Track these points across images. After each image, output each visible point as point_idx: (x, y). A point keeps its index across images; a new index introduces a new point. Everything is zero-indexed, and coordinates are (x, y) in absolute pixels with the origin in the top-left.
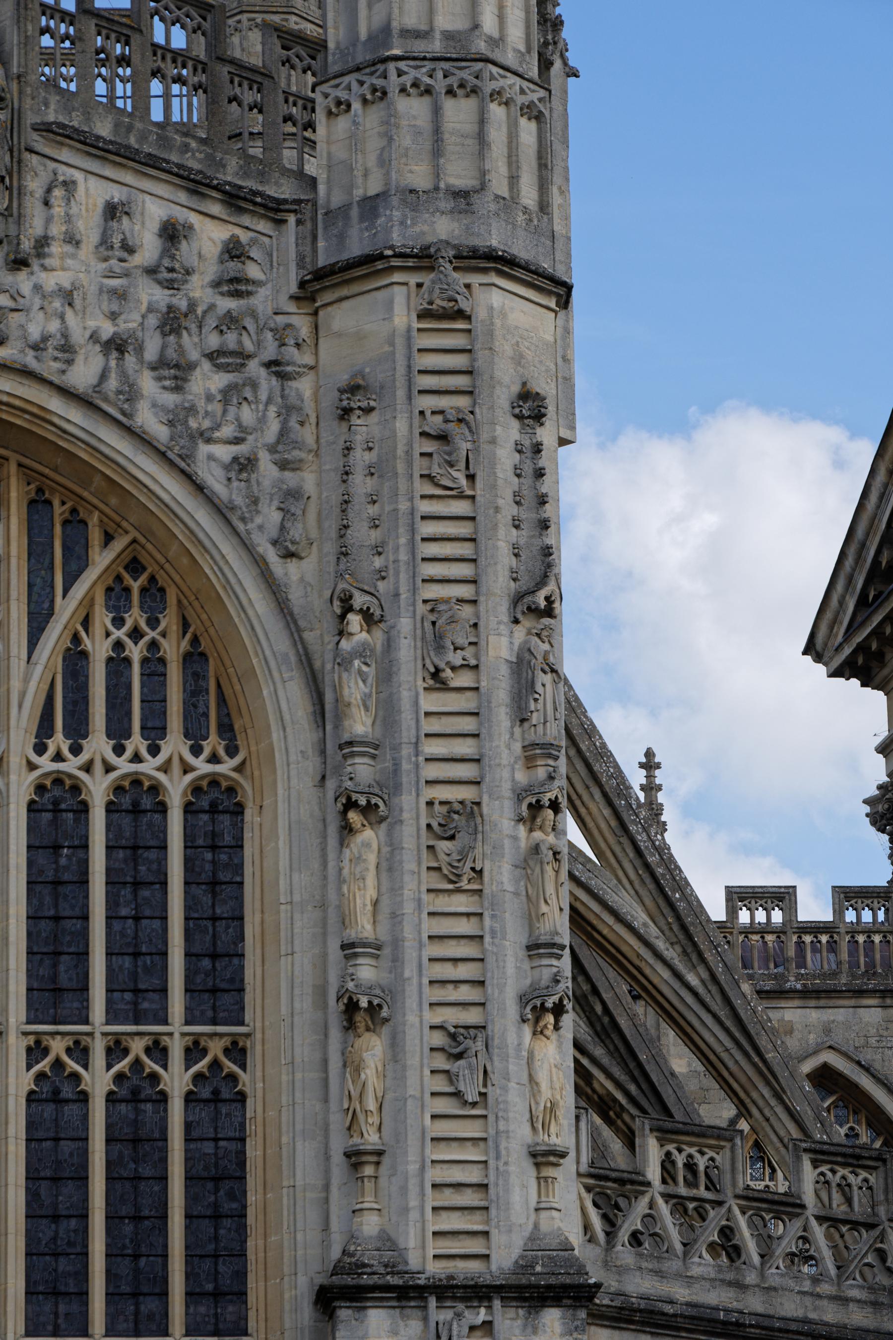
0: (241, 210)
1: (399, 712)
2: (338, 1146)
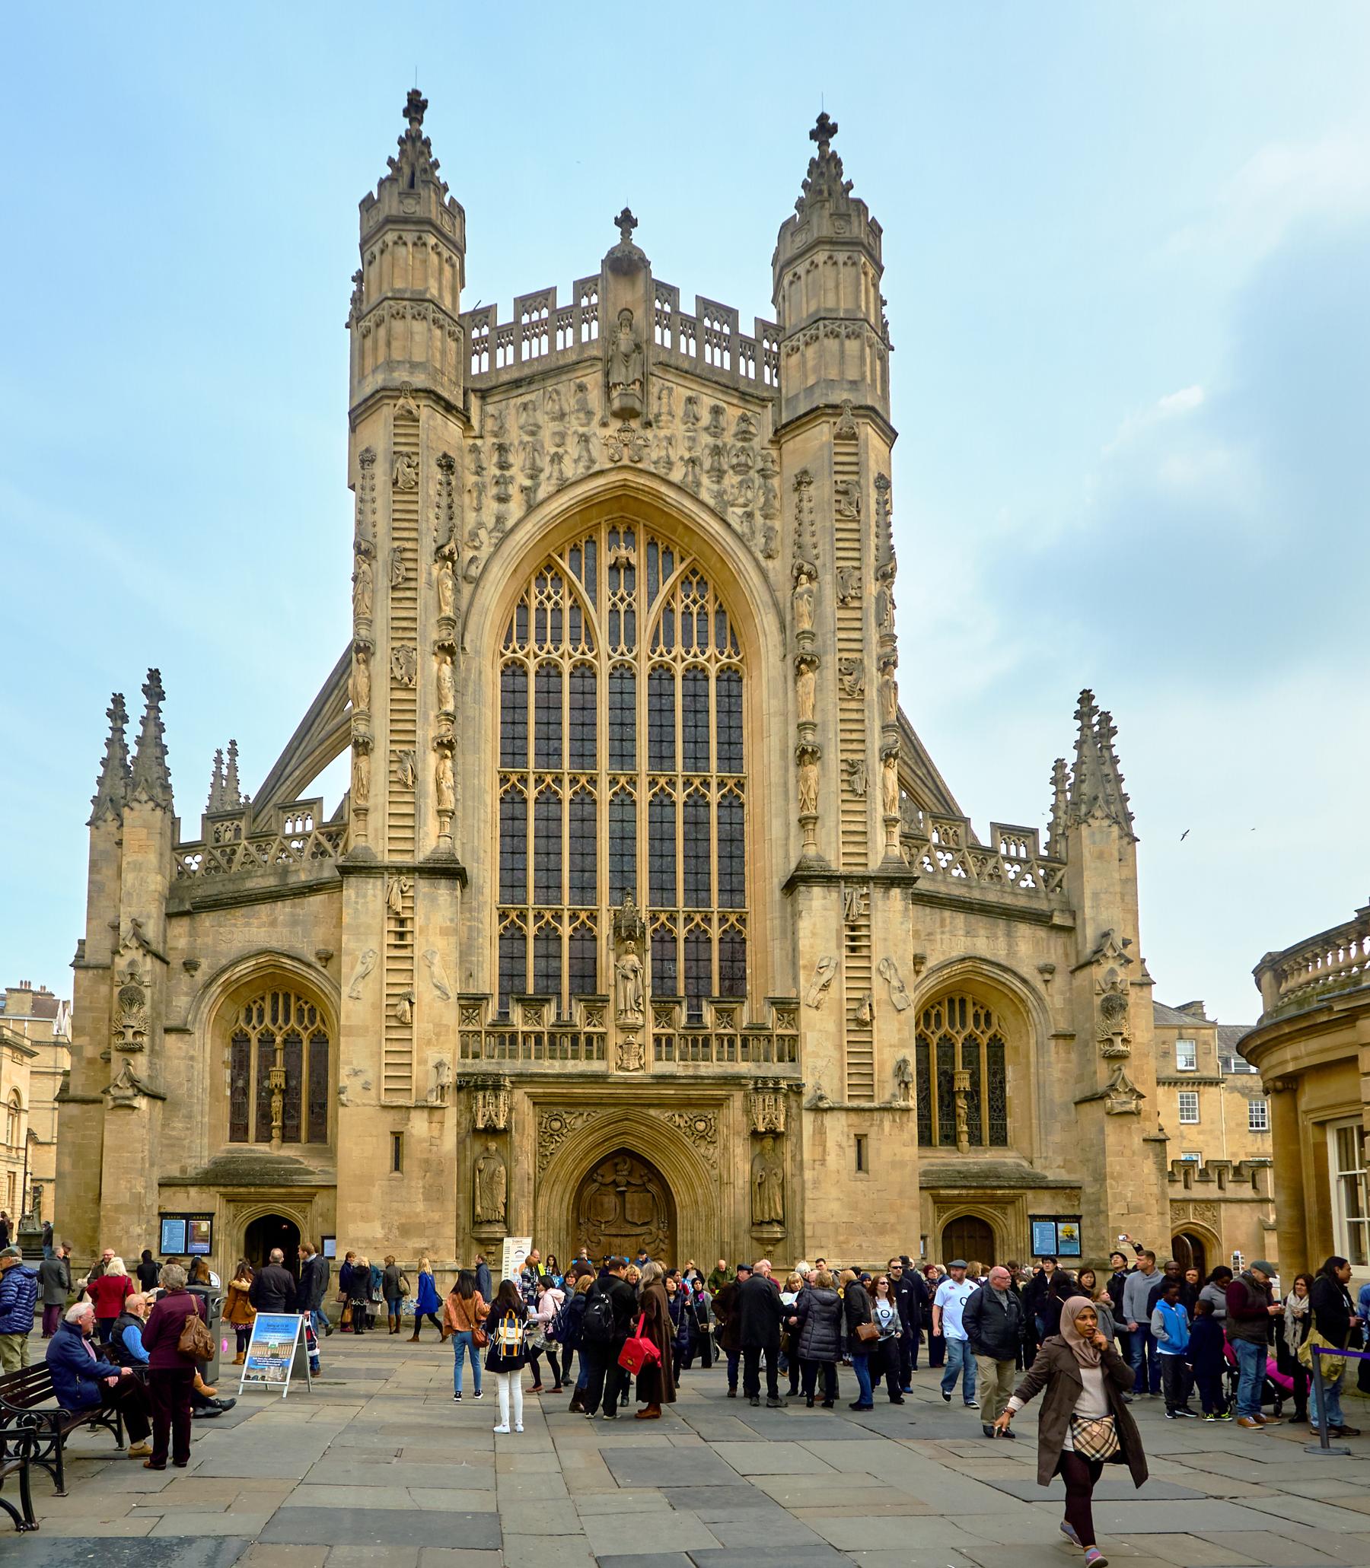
0: (747, 401)
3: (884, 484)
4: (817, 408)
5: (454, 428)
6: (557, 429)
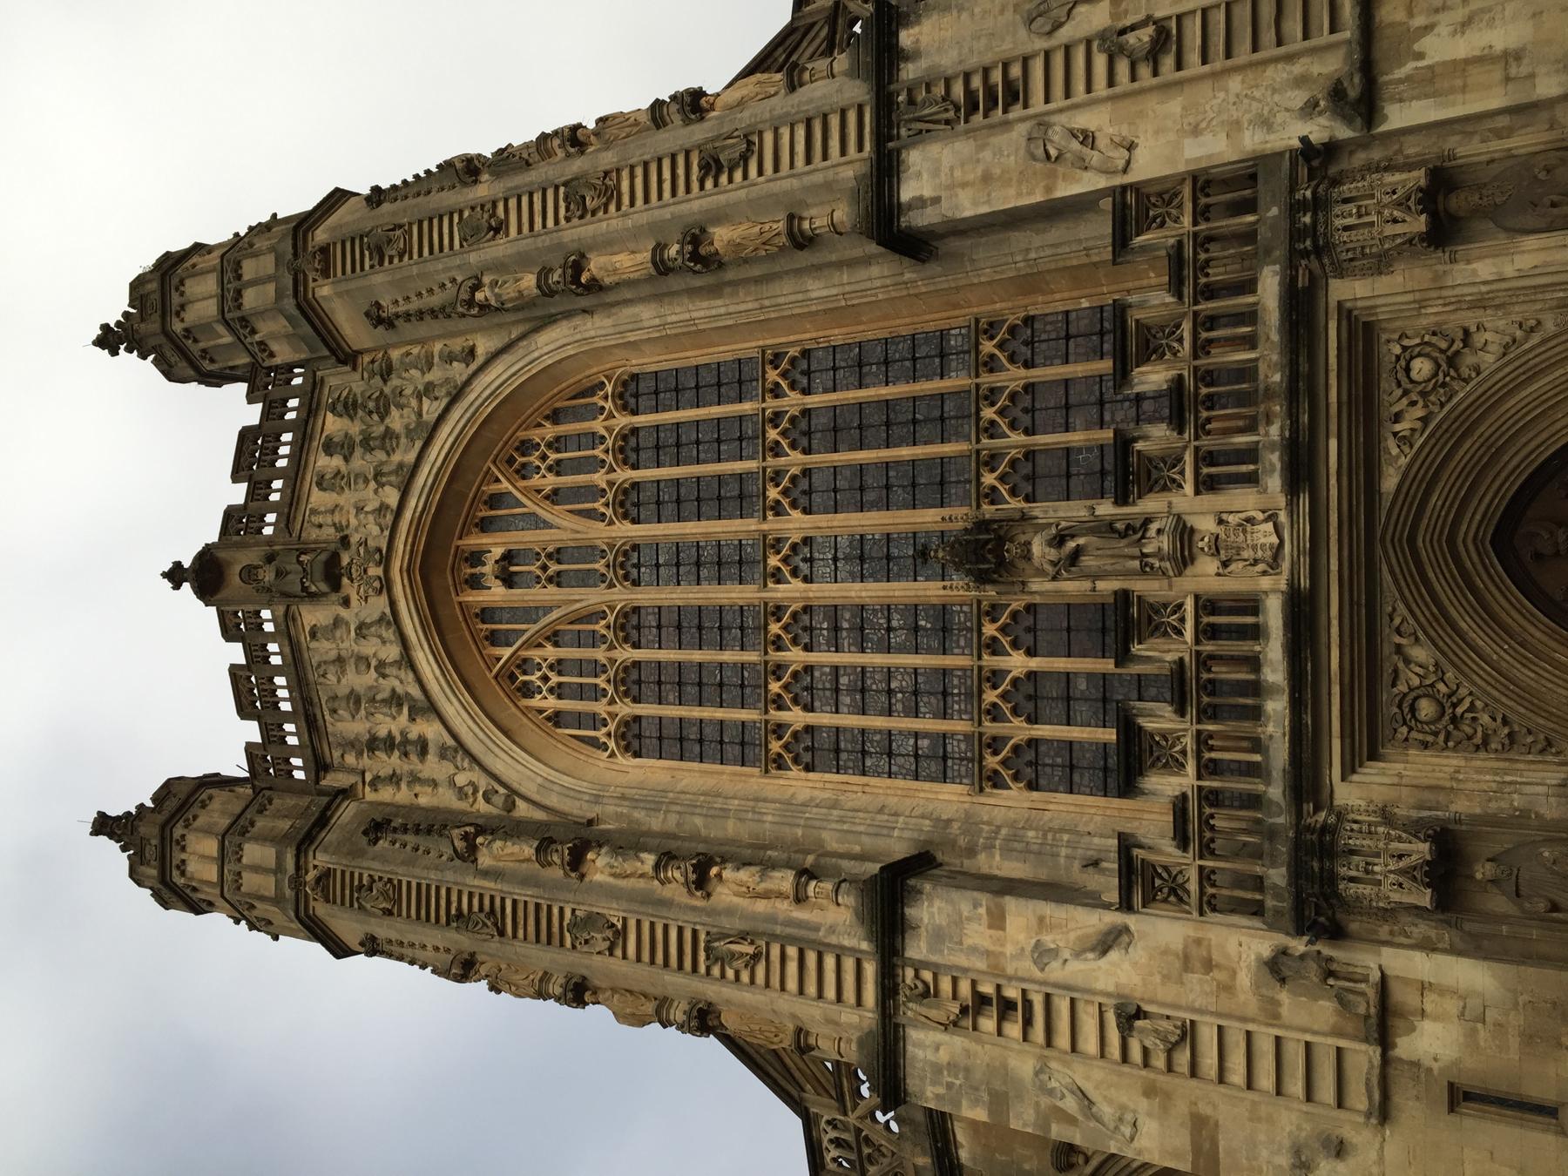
0: (319, 404)
1: (519, 253)
2: (804, 258)
4: (299, 306)
5: (347, 813)
6: (353, 667)
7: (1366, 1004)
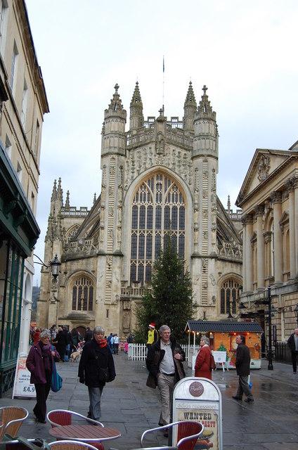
3: (214, 170)
5: (123, 158)
7: (115, 303)
